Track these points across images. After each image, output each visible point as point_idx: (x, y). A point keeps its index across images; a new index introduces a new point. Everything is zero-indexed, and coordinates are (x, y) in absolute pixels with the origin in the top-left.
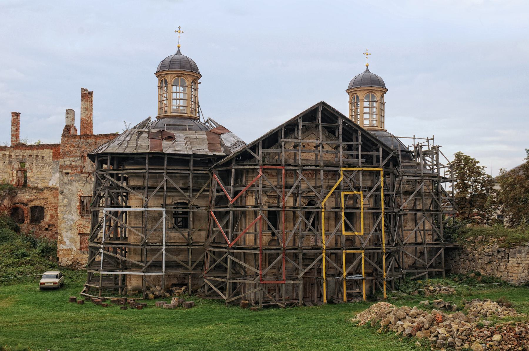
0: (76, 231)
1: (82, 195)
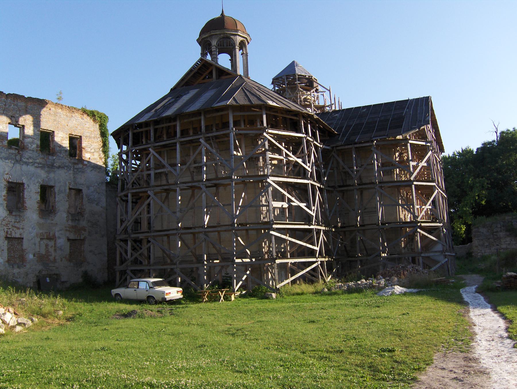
0: (3, 234)
1: (10, 181)
